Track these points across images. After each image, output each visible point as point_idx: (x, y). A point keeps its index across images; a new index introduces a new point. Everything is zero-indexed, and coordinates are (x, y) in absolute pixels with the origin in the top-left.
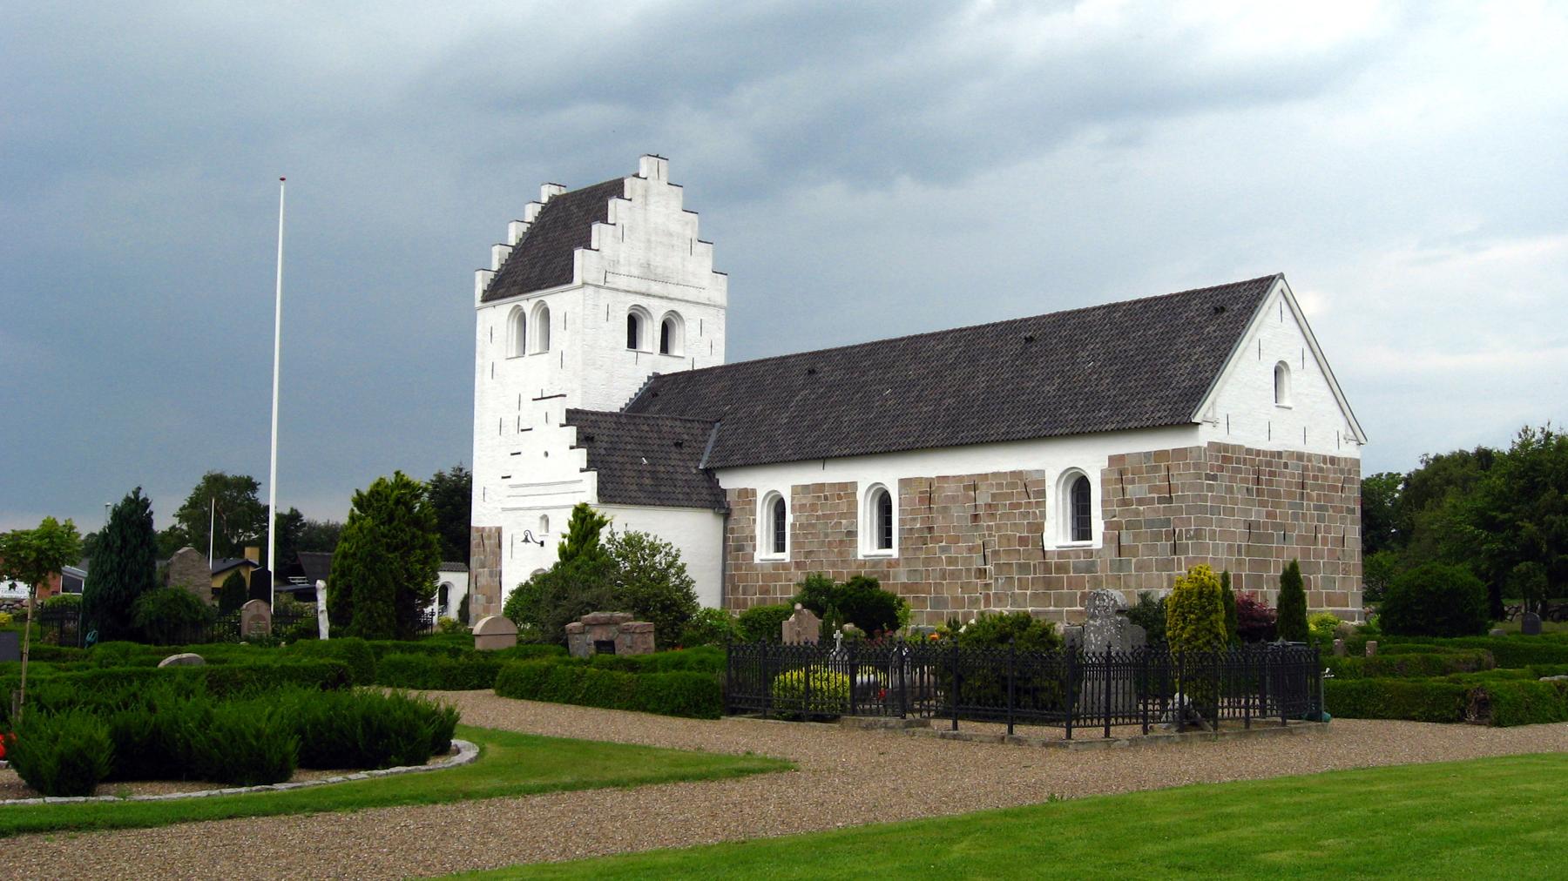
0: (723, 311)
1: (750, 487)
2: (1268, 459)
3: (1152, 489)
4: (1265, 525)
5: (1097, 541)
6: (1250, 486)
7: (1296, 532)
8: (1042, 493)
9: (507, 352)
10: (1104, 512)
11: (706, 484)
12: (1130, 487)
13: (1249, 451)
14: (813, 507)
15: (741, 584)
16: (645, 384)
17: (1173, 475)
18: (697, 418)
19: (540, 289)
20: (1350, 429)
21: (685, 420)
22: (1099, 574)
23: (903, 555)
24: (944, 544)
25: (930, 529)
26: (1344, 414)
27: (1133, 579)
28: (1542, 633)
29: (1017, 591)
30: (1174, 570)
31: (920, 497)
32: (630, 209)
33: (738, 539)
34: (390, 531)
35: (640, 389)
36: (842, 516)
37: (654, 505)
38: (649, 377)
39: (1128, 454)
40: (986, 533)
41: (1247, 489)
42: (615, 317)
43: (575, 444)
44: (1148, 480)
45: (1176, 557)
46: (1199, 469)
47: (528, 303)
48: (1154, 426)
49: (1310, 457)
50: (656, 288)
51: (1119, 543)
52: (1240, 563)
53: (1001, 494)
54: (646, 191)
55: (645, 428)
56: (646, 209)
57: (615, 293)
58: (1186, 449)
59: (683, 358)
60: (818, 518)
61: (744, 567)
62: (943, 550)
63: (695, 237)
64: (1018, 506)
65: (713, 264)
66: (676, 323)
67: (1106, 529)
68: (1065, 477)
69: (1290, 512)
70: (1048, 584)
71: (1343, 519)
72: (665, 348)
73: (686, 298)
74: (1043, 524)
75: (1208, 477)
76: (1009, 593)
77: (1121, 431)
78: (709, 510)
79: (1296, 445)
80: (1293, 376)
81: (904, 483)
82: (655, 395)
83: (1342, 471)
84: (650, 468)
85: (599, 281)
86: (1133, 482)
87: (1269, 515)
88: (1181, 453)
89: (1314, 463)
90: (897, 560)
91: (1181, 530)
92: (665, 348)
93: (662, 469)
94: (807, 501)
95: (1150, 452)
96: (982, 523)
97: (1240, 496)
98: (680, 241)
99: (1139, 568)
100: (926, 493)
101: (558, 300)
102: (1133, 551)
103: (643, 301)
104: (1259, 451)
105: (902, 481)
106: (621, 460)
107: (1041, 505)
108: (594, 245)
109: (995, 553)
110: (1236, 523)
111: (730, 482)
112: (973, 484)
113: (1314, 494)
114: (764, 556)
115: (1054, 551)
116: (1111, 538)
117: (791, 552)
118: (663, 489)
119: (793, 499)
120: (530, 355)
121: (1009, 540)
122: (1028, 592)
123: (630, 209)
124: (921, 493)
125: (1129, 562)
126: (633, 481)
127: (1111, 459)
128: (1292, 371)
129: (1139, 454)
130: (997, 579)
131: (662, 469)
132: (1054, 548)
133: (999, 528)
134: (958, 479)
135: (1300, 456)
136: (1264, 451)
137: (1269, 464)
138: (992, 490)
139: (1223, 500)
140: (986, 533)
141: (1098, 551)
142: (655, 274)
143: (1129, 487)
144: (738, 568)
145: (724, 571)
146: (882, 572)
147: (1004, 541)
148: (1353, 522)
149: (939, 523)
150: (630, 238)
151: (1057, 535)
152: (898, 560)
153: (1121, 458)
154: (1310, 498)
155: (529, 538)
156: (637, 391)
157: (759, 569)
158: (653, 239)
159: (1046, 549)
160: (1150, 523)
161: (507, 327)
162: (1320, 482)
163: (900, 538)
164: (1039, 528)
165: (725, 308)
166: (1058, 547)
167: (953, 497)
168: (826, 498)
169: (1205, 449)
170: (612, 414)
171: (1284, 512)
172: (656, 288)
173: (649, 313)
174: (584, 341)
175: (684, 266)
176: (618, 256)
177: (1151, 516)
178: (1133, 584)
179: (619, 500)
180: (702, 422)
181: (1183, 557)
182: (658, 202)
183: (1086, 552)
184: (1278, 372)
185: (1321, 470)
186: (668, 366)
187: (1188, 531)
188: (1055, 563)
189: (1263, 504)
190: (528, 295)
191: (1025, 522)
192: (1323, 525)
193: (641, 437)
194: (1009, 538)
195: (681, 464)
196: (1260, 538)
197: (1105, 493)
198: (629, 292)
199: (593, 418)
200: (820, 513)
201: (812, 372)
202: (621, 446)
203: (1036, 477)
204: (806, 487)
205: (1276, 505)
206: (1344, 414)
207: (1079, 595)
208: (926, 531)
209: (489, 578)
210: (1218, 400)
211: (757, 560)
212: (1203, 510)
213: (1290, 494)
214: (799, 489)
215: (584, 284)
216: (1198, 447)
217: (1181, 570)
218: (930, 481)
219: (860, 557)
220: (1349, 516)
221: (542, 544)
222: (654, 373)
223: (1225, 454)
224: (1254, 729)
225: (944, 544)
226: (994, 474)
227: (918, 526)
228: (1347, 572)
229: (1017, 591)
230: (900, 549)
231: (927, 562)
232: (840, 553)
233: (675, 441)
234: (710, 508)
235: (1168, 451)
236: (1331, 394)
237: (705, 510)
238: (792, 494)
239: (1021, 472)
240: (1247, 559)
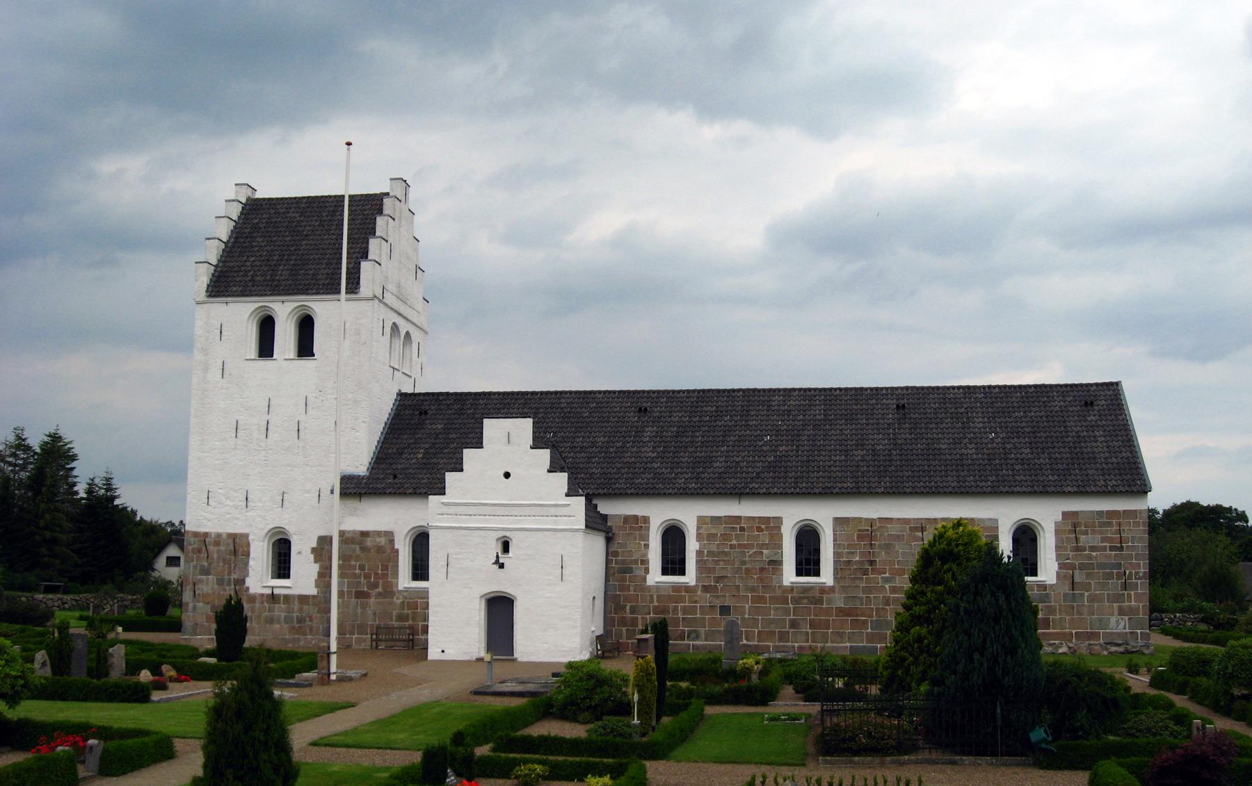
14: (725, 537)
17: (1124, 530)
22: (1053, 604)
23: (839, 583)
24: (887, 575)
25: (872, 563)
30: (1124, 602)
31: (858, 535)
33: (623, 562)
39: (1081, 511)
44: (1101, 533)
45: (1126, 593)
47: (285, 311)
58: (1136, 511)
60: (732, 547)
62: (886, 580)
77: (1082, 492)
81: (839, 522)
86: (1086, 533)
91: (1131, 573)
94: (719, 530)
95: (1103, 511)
99: (1092, 599)
102: (1087, 587)
116: (1065, 576)
119: (698, 528)
124: (859, 530)
125: (1082, 595)
127: (1065, 514)
129: (1093, 512)
141: (1052, 586)
143: (1082, 538)
146: (814, 597)
149: (881, 556)
152: (833, 587)
153: (1075, 514)
160: (1102, 566)
167: (898, 536)
168: (742, 529)
177: (1104, 560)
181: (1132, 593)
187: (1137, 573)
200: (734, 542)
204: (716, 520)
209: (216, 587)
214: (708, 520)
217: (1131, 602)
218: (871, 522)
227: (857, 559)
231: (867, 590)
232: (761, 579)
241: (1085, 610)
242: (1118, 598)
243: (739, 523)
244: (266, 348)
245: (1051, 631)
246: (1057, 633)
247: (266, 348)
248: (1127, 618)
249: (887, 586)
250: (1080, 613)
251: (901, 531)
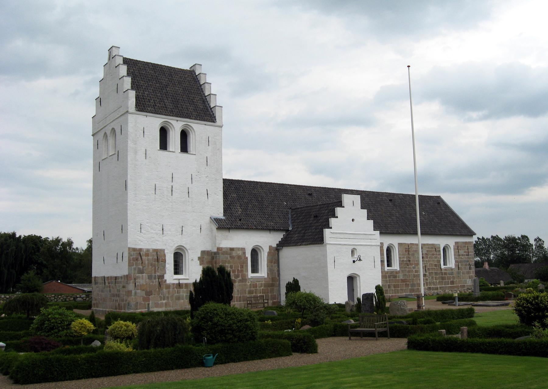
23: (401, 269)
24: (413, 266)
25: (409, 261)
29: (434, 281)
31: (405, 250)
62: (414, 268)
64: (433, 254)
67: (455, 262)
70: (443, 278)
81: (400, 244)
86: (460, 250)
90: (399, 271)
96: (424, 259)
105: (399, 244)
109: (428, 269)
124: (406, 248)
141: (454, 268)
146: (394, 275)
147: (431, 265)
152: (399, 271)
160: (465, 261)
188: (444, 272)
207: (450, 281)
209: (147, 280)
218: (408, 245)
225: (413, 266)
226: (427, 244)
227: (405, 259)
229: (434, 281)
231: (409, 272)
239: (434, 244)
242: (468, 273)
244: (164, 145)
247: (164, 145)
248: (471, 280)
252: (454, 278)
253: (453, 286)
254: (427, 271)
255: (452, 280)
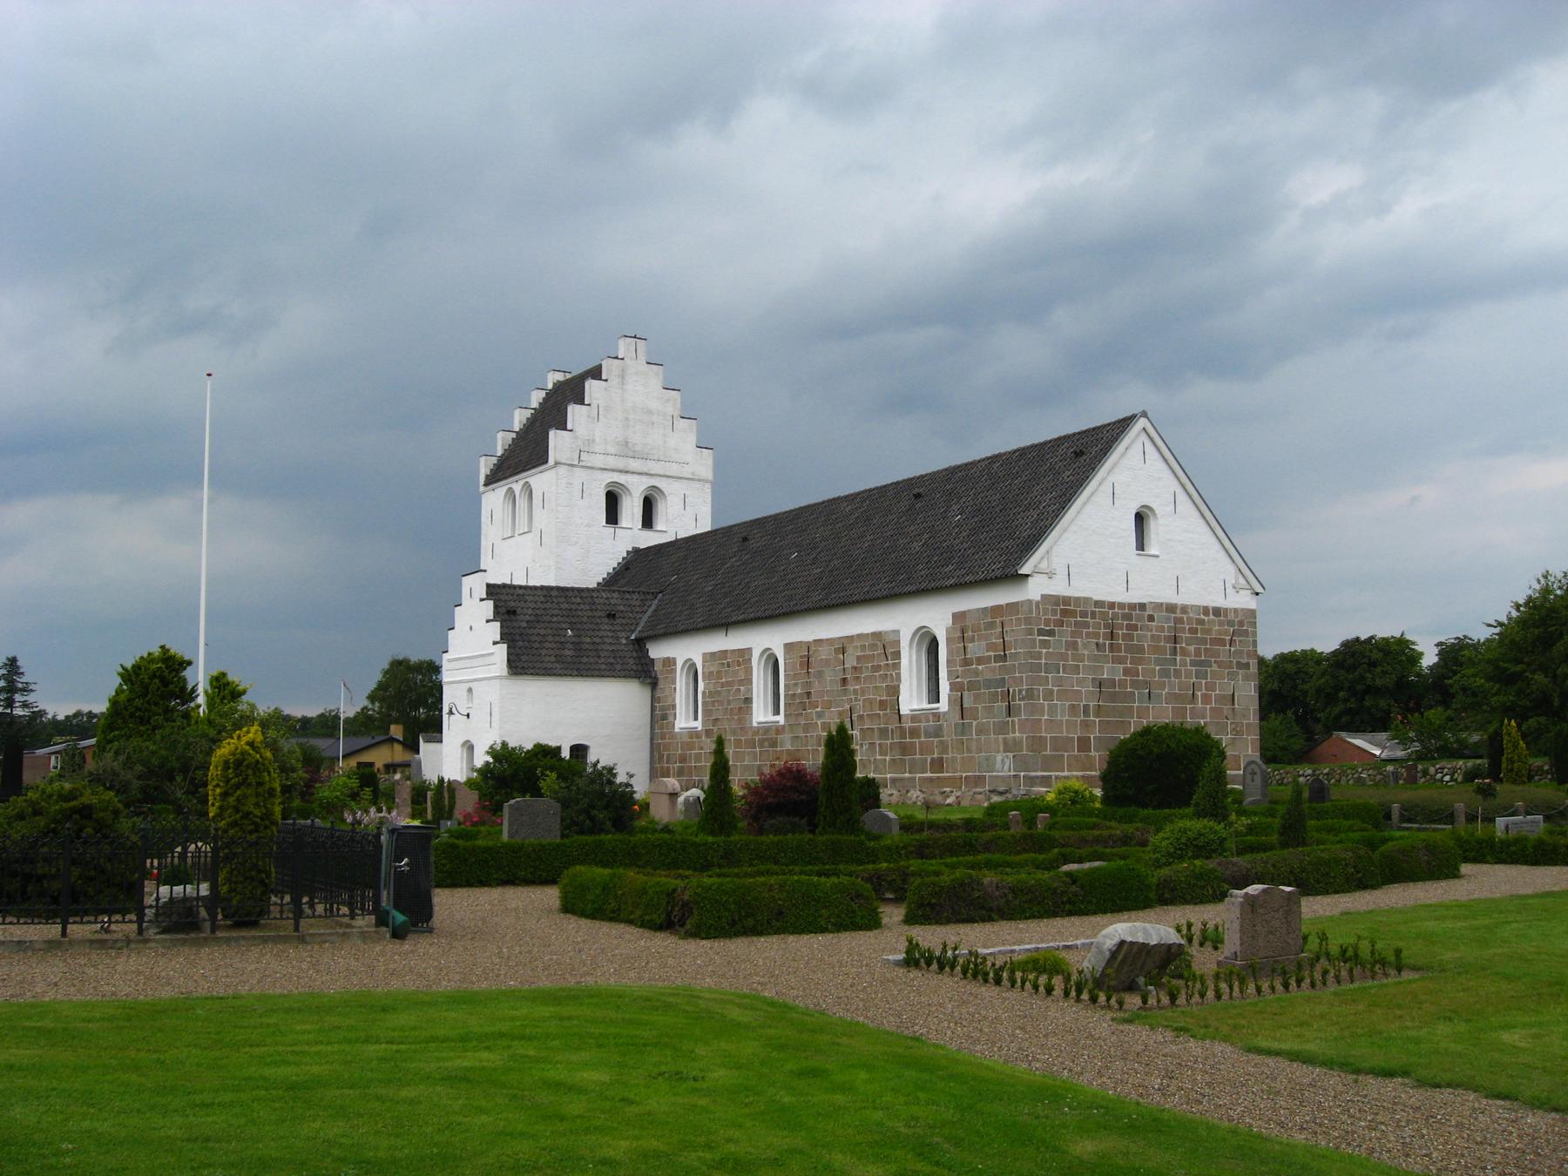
0: (708, 485)
1: (671, 656)
2: (1127, 611)
3: (990, 647)
4: (1122, 683)
5: (943, 705)
6: (1101, 641)
7: (1166, 690)
8: (897, 655)
9: (503, 532)
10: (949, 672)
11: (635, 654)
12: (971, 645)
13: (1098, 604)
15: (666, 753)
16: (624, 559)
17: (1007, 631)
18: (638, 590)
19: (524, 471)
20: (1240, 576)
21: (624, 592)
24: (819, 709)
25: (809, 694)
26: (1233, 561)
27: (974, 743)
28: (1332, 801)
29: (878, 757)
30: (1008, 733)
32: (605, 389)
33: (662, 708)
34: (143, 704)
35: (619, 564)
36: (741, 682)
37: (571, 675)
38: (628, 552)
39: (969, 611)
40: (853, 697)
41: (1097, 644)
42: (591, 495)
43: (492, 618)
45: (1010, 719)
46: (1030, 624)
48: (986, 579)
49: (1184, 609)
50: (635, 465)
51: (962, 705)
52: (1086, 725)
53: (864, 656)
54: (623, 370)
55: (579, 600)
56: (622, 388)
57: (590, 471)
58: (1017, 603)
59: (665, 532)
60: (723, 685)
61: (667, 736)
62: (820, 715)
63: (677, 413)
64: (876, 668)
65: (697, 441)
66: (658, 497)
67: (951, 690)
68: (919, 635)
69: (1157, 668)
70: (905, 749)
71: (1232, 676)
72: (648, 521)
73: (668, 474)
74: (899, 686)
75: (1041, 632)
76: (872, 759)
78: (634, 680)
79: (1167, 596)
80: (1161, 521)
81: (789, 647)
82: (627, 569)
83: (1231, 623)
84: (574, 639)
85: (573, 460)
86: (973, 640)
87: (1126, 672)
88: (1013, 607)
89: (1191, 615)
91: (1014, 690)
92: (648, 521)
93: (588, 640)
97: (1086, 653)
98: (661, 418)
99: (979, 732)
100: (804, 656)
101: (540, 480)
103: (621, 478)
104: (1114, 603)
105: (786, 645)
106: (542, 632)
107: (897, 666)
108: (569, 427)
109: (861, 717)
110: (1080, 682)
111: (658, 651)
112: (842, 646)
113: (1192, 648)
114: (762, 719)
115: (908, 715)
116: (955, 700)
117: (703, 720)
118: (585, 660)
119: (703, 666)
120: (519, 535)
121: (871, 703)
122: (888, 758)
123: (605, 389)
124: (801, 657)
126: (552, 652)
128: (1159, 516)
129: (978, 609)
130: (862, 745)
131: (588, 640)
132: (908, 712)
133: (863, 691)
134: (830, 641)
135: (1171, 608)
136: (1119, 603)
137: (1127, 617)
138: (857, 652)
139: (1064, 657)
140: (853, 697)
141: (945, 713)
142: (635, 451)
144: (663, 737)
145: (652, 739)
147: (867, 705)
148: (1246, 678)
150: (605, 417)
151: (912, 699)
152: (784, 726)
154: (1184, 653)
155: (454, 710)
156: (616, 566)
157: (678, 737)
158: (631, 417)
159: (901, 713)
160: (988, 683)
161: (503, 508)
162: (1199, 635)
163: (785, 704)
164: (894, 691)
165: (711, 482)
166: (912, 711)
169: (1037, 603)
170: (588, 590)
171: (1150, 668)
172: (635, 465)
173: (628, 490)
174: (558, 518)
175: (665, 442)
176: (594, 435)
177: (989, 676)
178: (974, 748)
179: (532, 671)
180: (643, 593)
181: (1016, 719)
182: (637, 381)
183: (935, 715)
184: (1140, 519)
185: (1201, 622)
186: (648, 539)
187: (1020, 691)
188: (909, 728)
189: (1121, 660)
190: (517, 477)
191: (884, 685)
192: (1204, 682)
193: (570, 610)
194: (870, 702)
195: (610, 634)
196: (1113, 697)
197: (950, 652)
198: (606, 469)
199: (521, 592)
200: (724, 680)
201: (745, 539)
202: (545, 618)
203: (892, 637)
204: (713, 654)
205: (1140, 661)
206: (1233, 561)
207: (929, 760)
208: (805, 696)
210: (1054, 550)
211: (677, 730)
212: (1038, 668)
213: (1156, 649)
215: (557, 463)
216: (1028, 600)
217: (1015, 733)
218: (808, 645)
219: (755, 724)
220: (1240, 671)
221: (468, 715)
222: (633, 548)
223: (1065, 610)
224: (220, 936)
225: (819, 709)
227: (799, 691)
228: (1237, 732)
230: (785, 715)
232: (739, 719)
233: (608, 612)
234: (636, 677)
235: (1002, 606)
236: (1214, 540)
237: (629, 680)
238: (703, 662)
240: (1097, 720)
241: (974, 746)
242: (1002, 728)
243: (726, 658)
245: (945, 774)
246: (949, 778)
248: (1011, 755)
249: (819, 722)
250: (969, 751)
251: (829, 655)
252: (944, 747)
253: (938, 778)
254: (855, 724)
255: (935, 756)
